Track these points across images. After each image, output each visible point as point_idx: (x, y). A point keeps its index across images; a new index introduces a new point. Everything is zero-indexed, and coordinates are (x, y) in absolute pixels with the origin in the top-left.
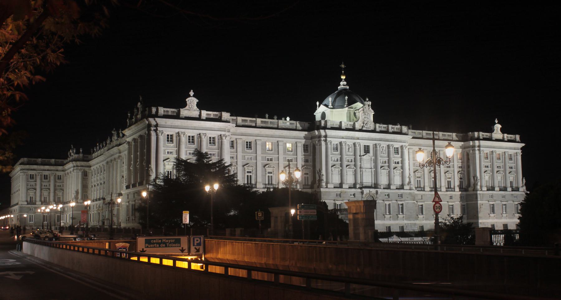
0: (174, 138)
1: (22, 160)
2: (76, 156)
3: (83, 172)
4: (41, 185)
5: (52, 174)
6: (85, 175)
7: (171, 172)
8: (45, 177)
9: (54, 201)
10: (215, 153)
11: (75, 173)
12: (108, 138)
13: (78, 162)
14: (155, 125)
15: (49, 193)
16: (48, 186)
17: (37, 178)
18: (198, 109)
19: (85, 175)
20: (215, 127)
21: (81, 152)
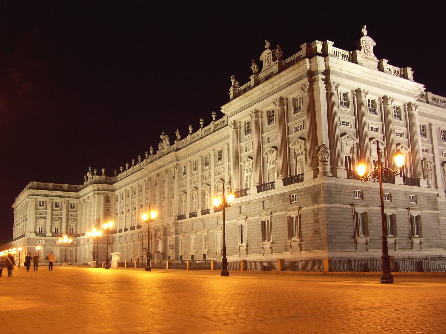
0: (351, 100)
1: (31, 184)
2: (97, 177)
3: (105, 197)
4: (52, 214)
5: (64, 202)
6: (107, 201)
7: (349, 157)
8: (56, 204)
9: (67, 232)
10: (403, 133)
11: (96, 198)
12: (150, 147)
13: (100, 185)
14: (323, 72)
15: (61, 223)
16: (60, 215)
17: (48, 205)
18: (375, 58)
19: (107, 200)
20: (403, 89)
21: (103, 173)
